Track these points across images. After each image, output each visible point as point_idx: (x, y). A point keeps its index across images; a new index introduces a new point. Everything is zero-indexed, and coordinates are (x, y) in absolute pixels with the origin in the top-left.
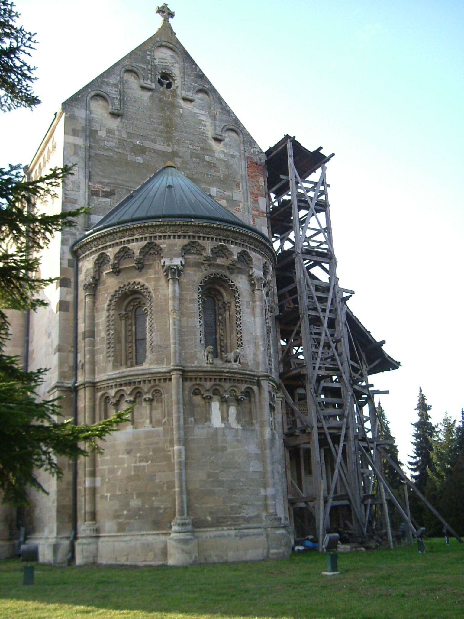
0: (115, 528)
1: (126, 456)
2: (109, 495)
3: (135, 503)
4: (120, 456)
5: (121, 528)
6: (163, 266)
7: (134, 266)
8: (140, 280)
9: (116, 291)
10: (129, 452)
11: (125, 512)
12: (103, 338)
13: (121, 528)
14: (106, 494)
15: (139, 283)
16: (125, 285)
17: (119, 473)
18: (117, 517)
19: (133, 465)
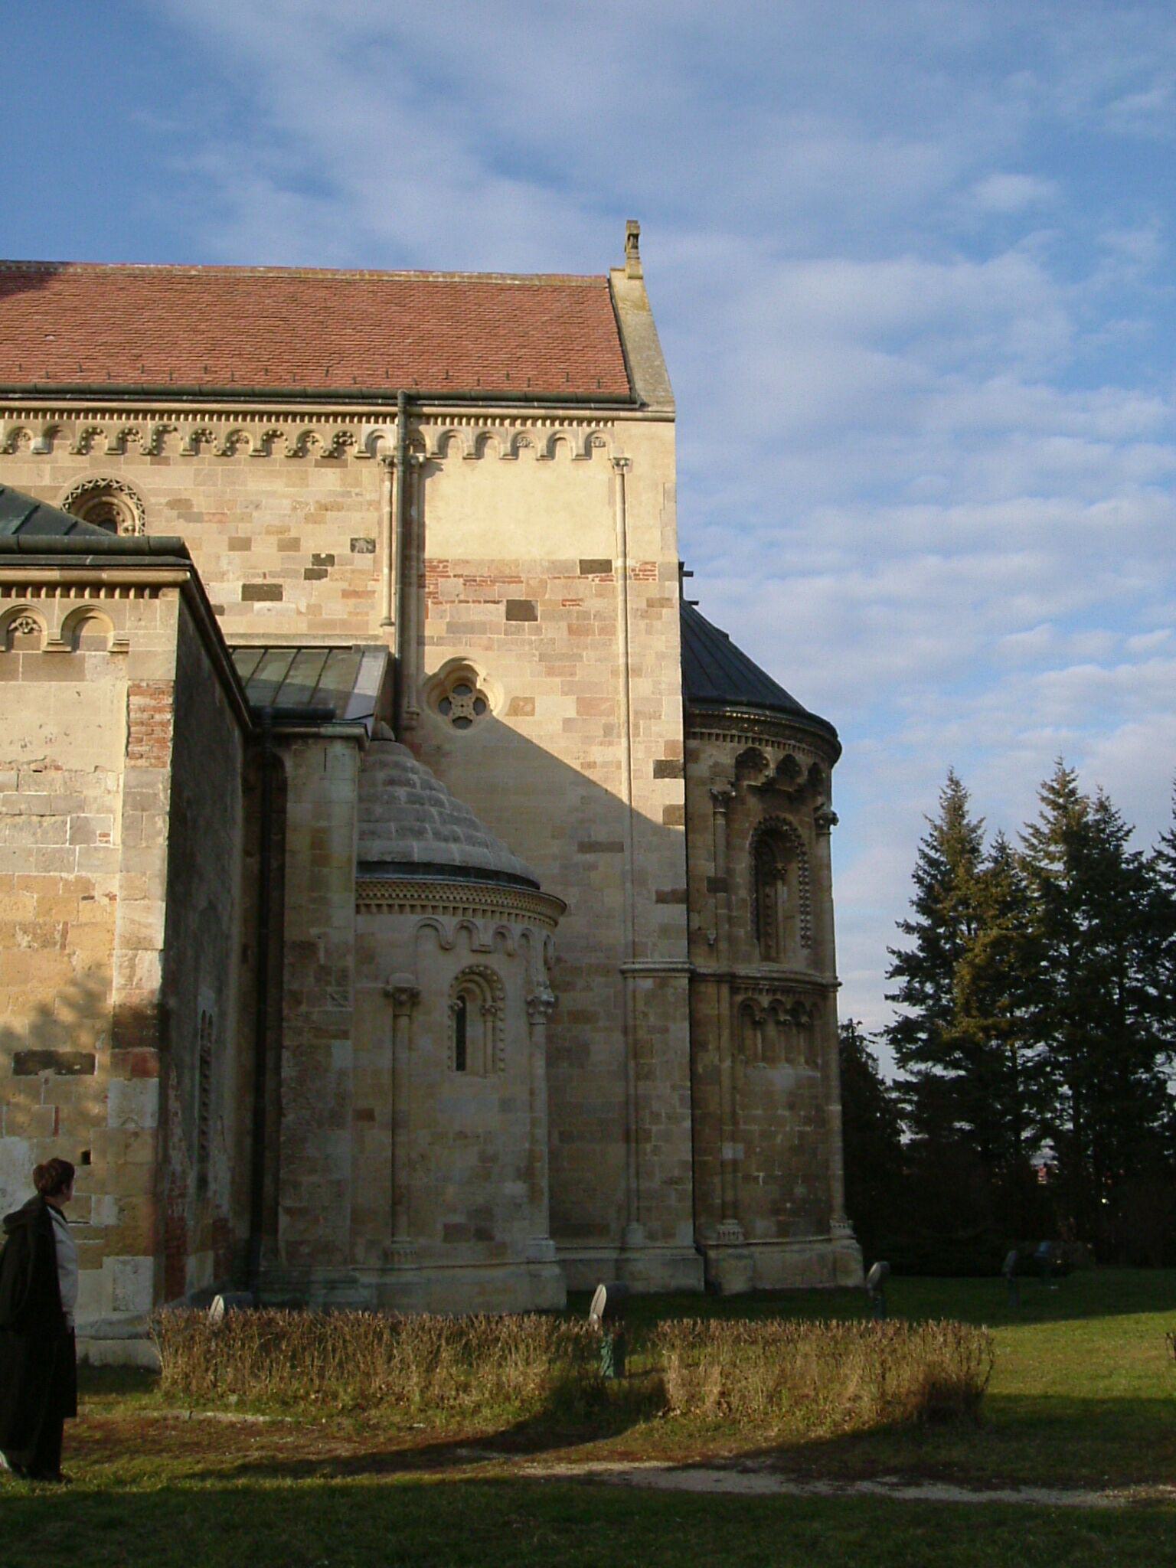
0: (774, 1229)
1: (787, 1113)
2: (761, 1174)
3: (800, 1190)
4: (780, 1112)
5: (783, 1230)
6: (817, 809)
7: (789, 793)
8: (790, 817)
9: (760, 823)
10: (791, 1107)
11: (788, 1205)
12: (744, 900)
13: (783, 1230)
14: (756, 1174)
15: (790, 824)
16: (771, 818)
17: (779, 1139)
18: (776, 1211)
19: (797, 1128)
